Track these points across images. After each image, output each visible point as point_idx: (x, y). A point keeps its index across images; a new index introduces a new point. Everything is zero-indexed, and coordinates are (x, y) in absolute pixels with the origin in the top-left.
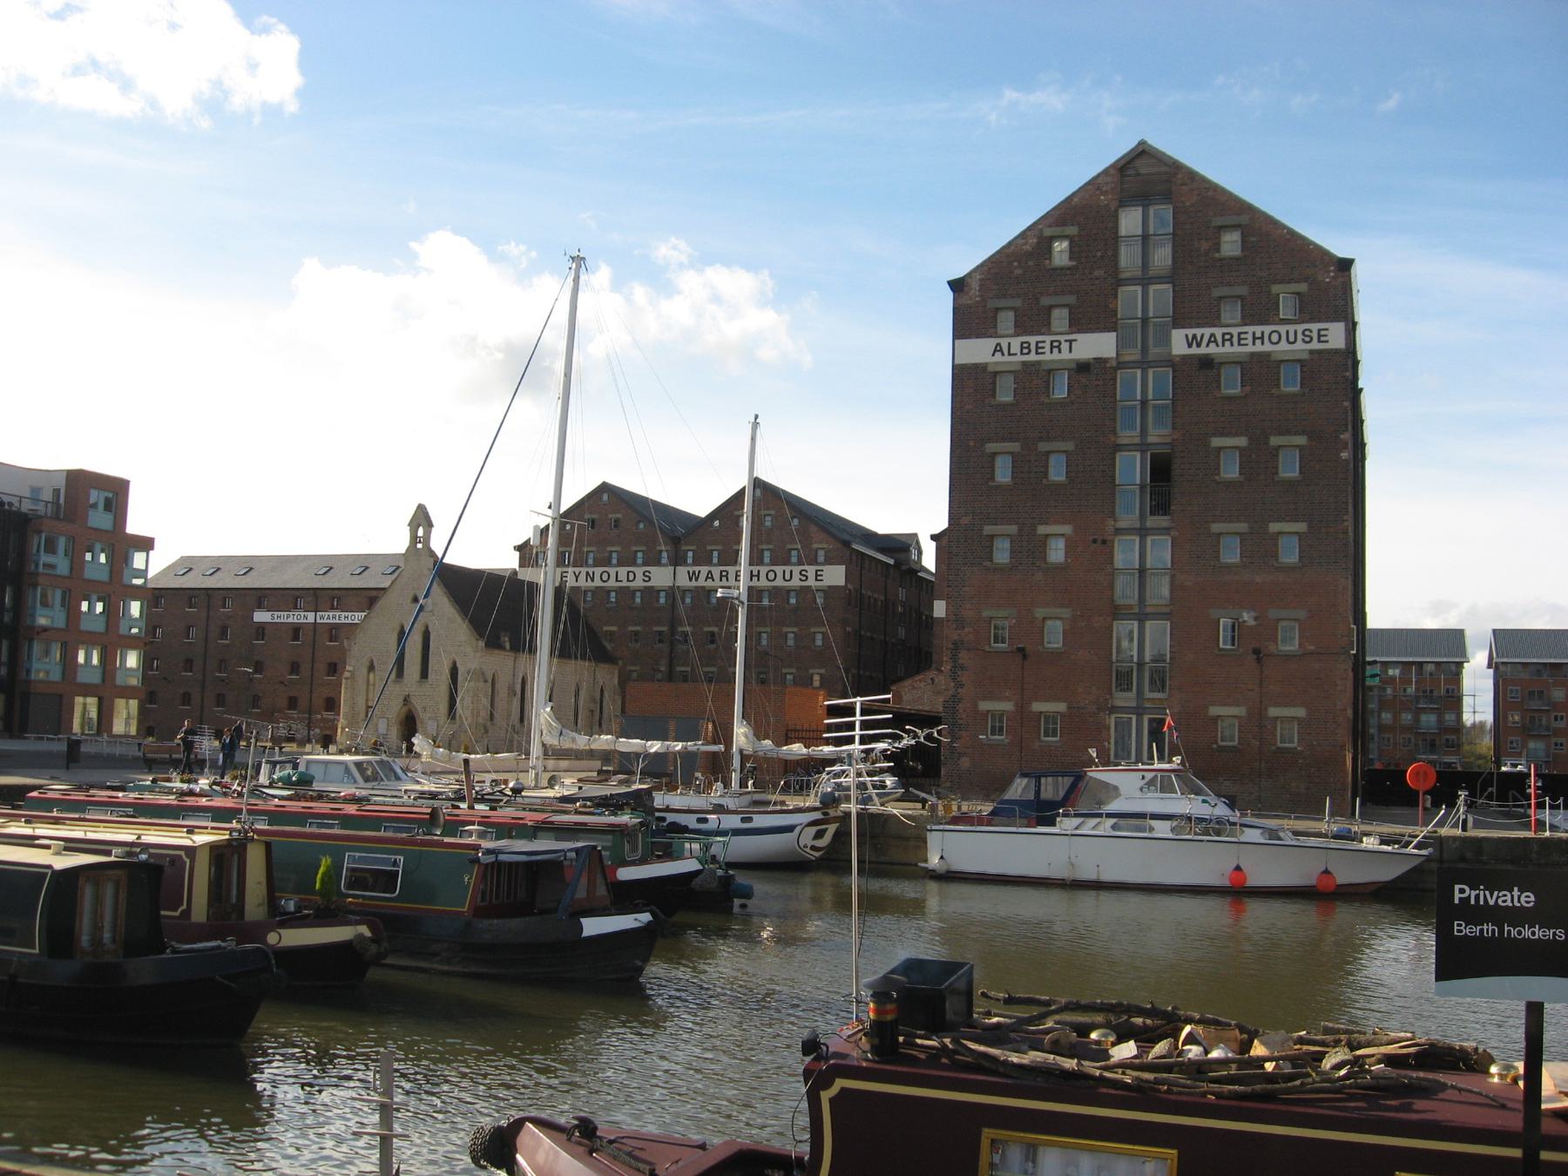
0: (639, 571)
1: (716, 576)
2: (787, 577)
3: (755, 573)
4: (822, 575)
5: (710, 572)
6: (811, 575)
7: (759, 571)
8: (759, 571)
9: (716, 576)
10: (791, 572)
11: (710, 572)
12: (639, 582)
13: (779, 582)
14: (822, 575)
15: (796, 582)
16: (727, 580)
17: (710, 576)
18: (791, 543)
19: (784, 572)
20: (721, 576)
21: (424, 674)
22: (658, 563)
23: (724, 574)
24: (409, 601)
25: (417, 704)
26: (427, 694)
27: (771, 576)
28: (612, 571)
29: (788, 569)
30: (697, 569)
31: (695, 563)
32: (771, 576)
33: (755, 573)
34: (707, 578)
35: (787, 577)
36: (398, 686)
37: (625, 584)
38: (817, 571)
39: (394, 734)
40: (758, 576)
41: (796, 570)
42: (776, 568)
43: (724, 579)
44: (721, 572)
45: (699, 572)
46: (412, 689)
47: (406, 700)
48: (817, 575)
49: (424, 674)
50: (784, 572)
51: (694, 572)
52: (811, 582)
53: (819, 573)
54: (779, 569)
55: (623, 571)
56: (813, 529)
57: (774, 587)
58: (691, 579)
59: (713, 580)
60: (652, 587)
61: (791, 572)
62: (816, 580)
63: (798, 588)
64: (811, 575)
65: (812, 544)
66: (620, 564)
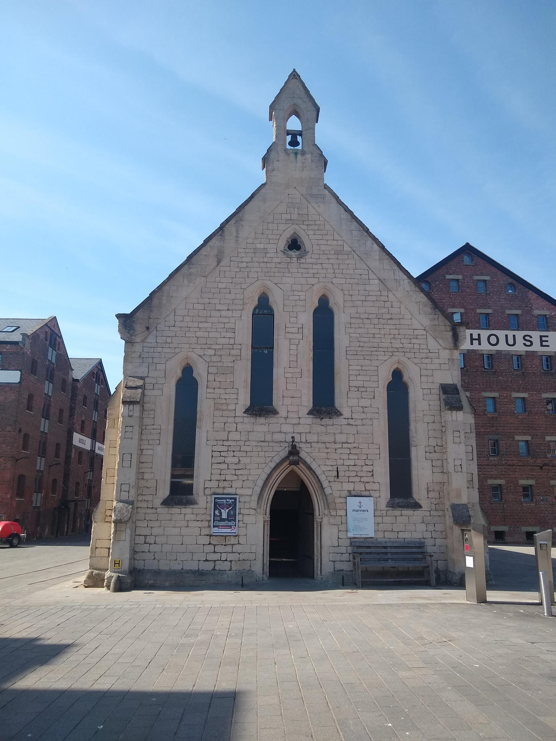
2: (511, 342)
3: (475, 336)
4: (547, 341)
7: (479, 335)
8: (479, 335)
10: (514, 336)
13: (502, 346)
14: (547, 341)
15: (520, 348)
18: (510, 309)
19: (506, 336)
24: (283, 244)
26: (341, 438)
27: (493, 340)
29: (510, 333)
32: (493, 340)
33: (475, 336)
35: (511, 342)
36: (261, 420)
38: (541, 337)
40: (479, 339)
41: (520, 335)
46: (300, 429)
47: (294, 451)
48: (542, 341)
50: (506, 336)
52: (536, 347)
53: (544, 339)
54: (501, 334)
56: (532, 295)
57: (499, 352)
61: (514, 336)
62: (542, 345)
63: (524, 353)
65: (532, 309)
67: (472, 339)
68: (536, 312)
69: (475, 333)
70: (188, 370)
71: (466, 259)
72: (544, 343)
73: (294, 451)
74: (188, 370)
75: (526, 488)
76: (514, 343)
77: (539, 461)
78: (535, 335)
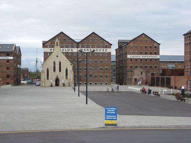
0: (70, 49)
1: (86, 50)
6: (105, 50)
9: (86, 50)
12: (70, 51)
13: (99, 51)
15: (102, 51)
17: (85, 50)
21: (60, 71)
22: (74, 47)
25: (59, 77)
27: (97, 50)
28: (64, 49)
29: (100, 49)
30: (82, 49)
31: (81, 47)
37: (67, 51)
39: (54, 83)
41: (102, 49)
47: (57, 76)
49: (60, 71)
52: (105, 51)
54: (98, 49)
55: (67, 49)
56: (105, 42)
60: (73, 52)
64: (105, 50)
66: (66, 47)
68: (105, 45)
70: (48, 69)
71: (93, 35)
73: (57, 76)
74: (48, 69)
75: (101, 76)
77: (103, 71)
78: (105, 49)
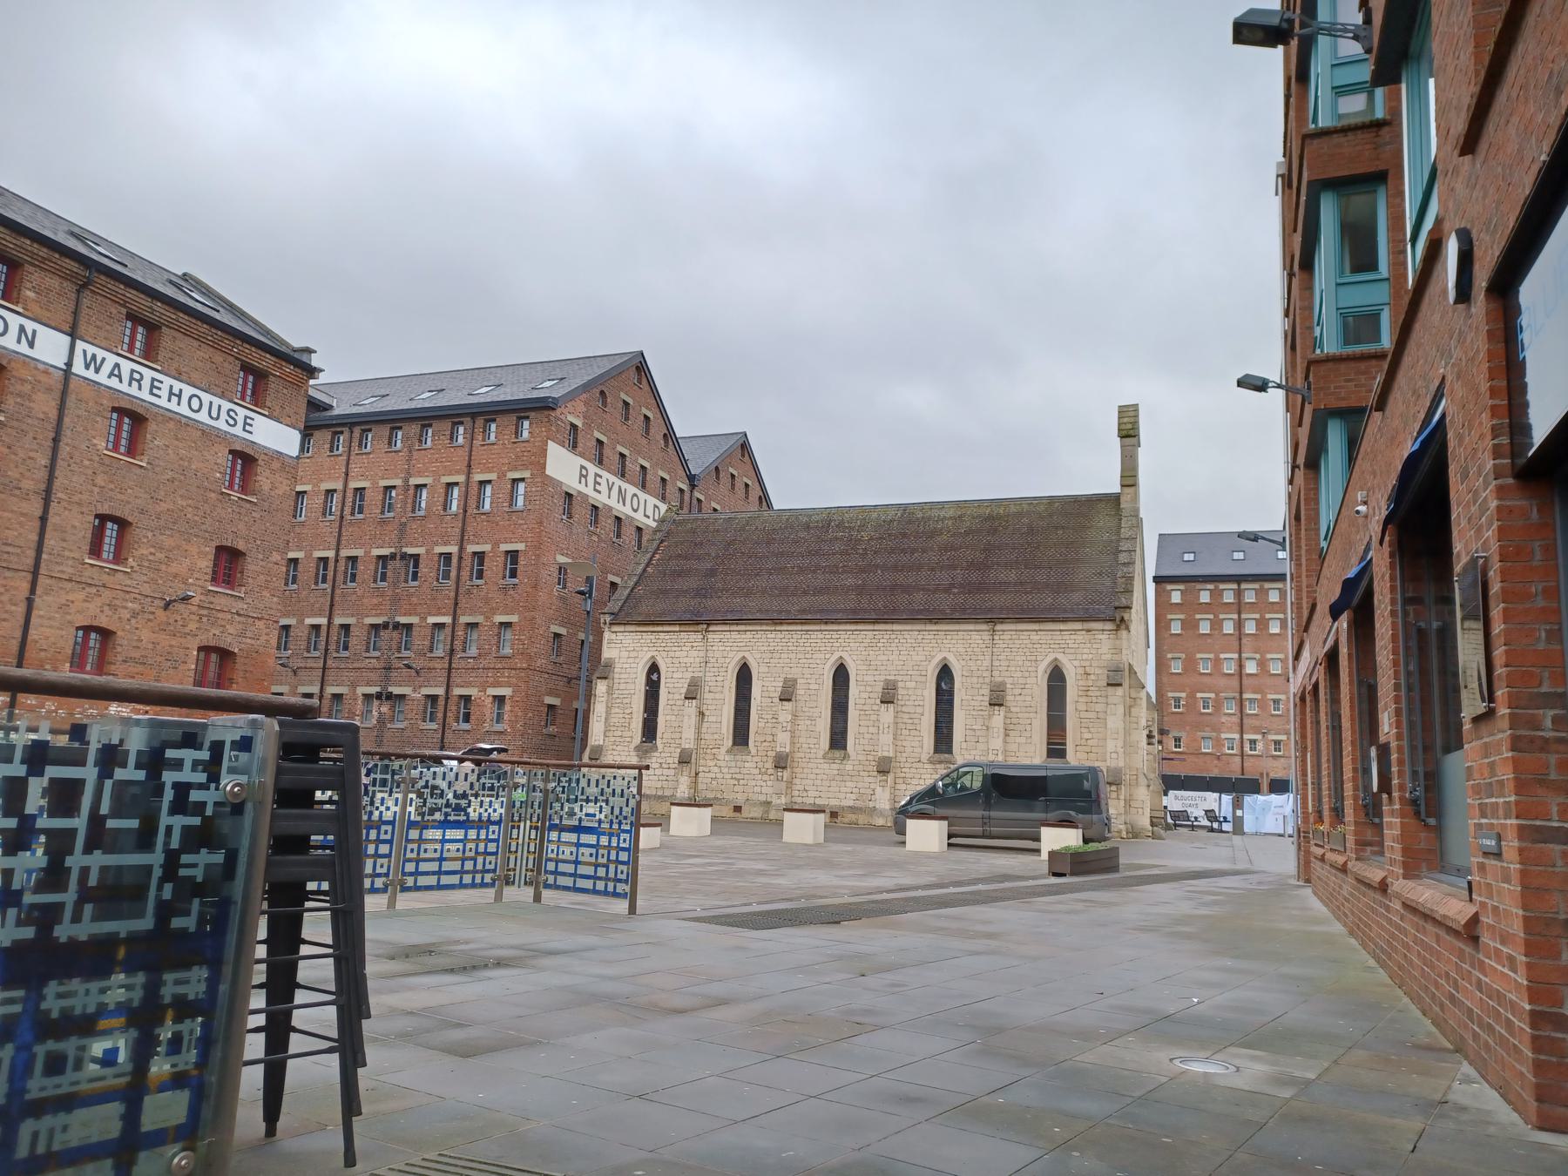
2: (214, 414)
4: (251, 425)
5: (117, 365)
7: (181, 391)
8: (181, 391)
10: (220, 406)
11: (117, 365)
14: (251, 425)
16: (140, 389)
17: (116, 372)
20: (132, 378)
23: (136, 376)
30: (100, 353)
33: (176, 391)
34: (111, 375)
35: (214, 414)
40: (179, 396)
42: (206, 397)
43: (135, 384)
44: (133, 371)
45: (104, 360)
50: (211, 403)
51: (94, 357)
58: (87, 367)
59: (121, 381)
61: (220, 406)
62: (244, 430)
67: (171, 393)
69: (177, 386)
72: (248, 428)
76: (217, 418)
